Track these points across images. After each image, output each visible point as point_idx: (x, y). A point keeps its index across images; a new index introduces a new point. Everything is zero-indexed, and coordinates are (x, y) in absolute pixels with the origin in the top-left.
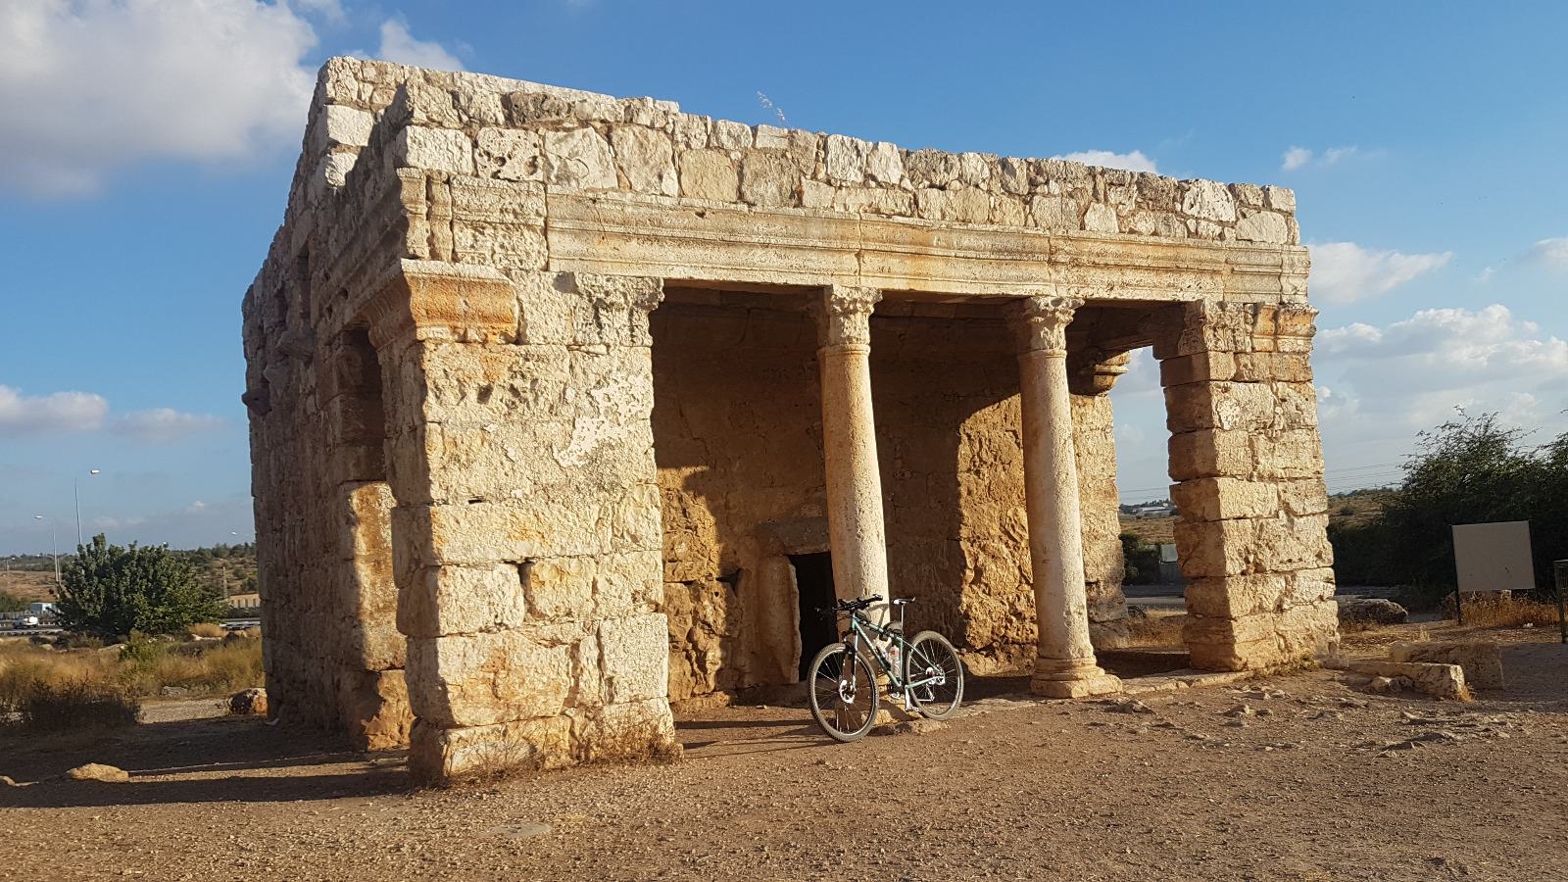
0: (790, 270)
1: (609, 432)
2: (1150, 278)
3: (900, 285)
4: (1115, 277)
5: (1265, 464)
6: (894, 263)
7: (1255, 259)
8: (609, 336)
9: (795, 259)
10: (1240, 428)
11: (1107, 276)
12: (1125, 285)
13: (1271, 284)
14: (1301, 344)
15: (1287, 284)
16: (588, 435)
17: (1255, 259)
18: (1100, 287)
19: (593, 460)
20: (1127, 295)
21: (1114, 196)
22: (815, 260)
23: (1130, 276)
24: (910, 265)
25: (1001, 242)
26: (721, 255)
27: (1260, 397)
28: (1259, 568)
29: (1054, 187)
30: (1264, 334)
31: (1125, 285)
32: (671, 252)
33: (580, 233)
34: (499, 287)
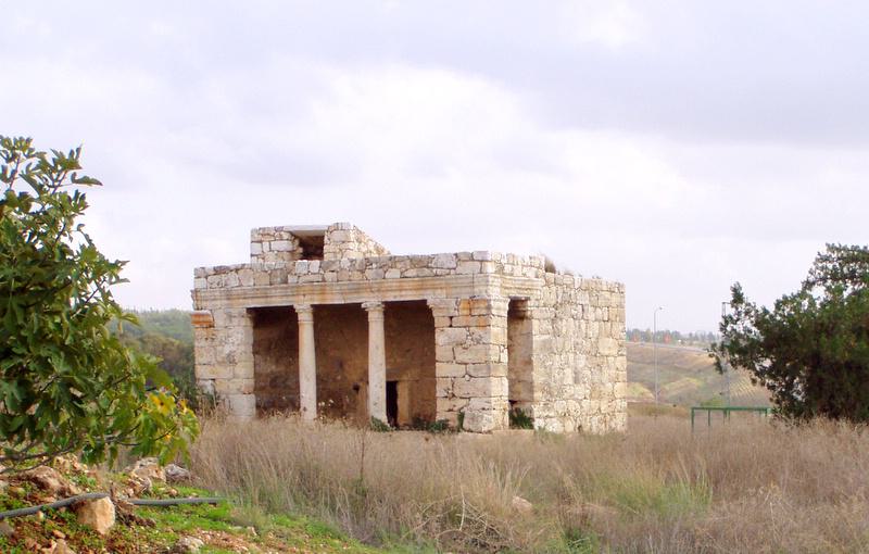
0: (283, 302)
1: (234, 348)
2: (410, 293)
3: (316, 303)
4: (397, 293)
5: (460, 358)
6: (316, 297)
7: (460, 281)
8: (235, 324)
9: (284, 299)
10: (449, 344)
11: (393, 294)
12: (401, 296)
13: (468, 290)
14: (484, 312)
15: (476, 290)
16: (227, 349)
17: (460, 281)
18: (391, 298)
19: (229, 355)
20: (402, 299)
21: (399, 265)
22: (291, 299)
23: (403, 293)
24: (320, 297)
25: (351, 287)
26: (262, 300)
27: (458, 333)
28: (454, 395)
29: (374, 266)
30: (464, 309)
31: (401, 296)
32: (250, 301)
33: (228, 299)
34: (208, 315)
